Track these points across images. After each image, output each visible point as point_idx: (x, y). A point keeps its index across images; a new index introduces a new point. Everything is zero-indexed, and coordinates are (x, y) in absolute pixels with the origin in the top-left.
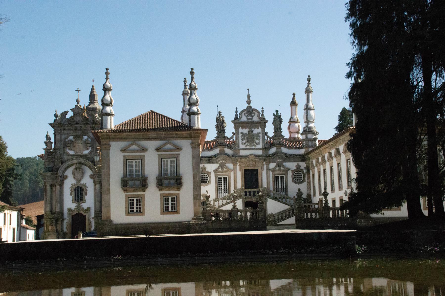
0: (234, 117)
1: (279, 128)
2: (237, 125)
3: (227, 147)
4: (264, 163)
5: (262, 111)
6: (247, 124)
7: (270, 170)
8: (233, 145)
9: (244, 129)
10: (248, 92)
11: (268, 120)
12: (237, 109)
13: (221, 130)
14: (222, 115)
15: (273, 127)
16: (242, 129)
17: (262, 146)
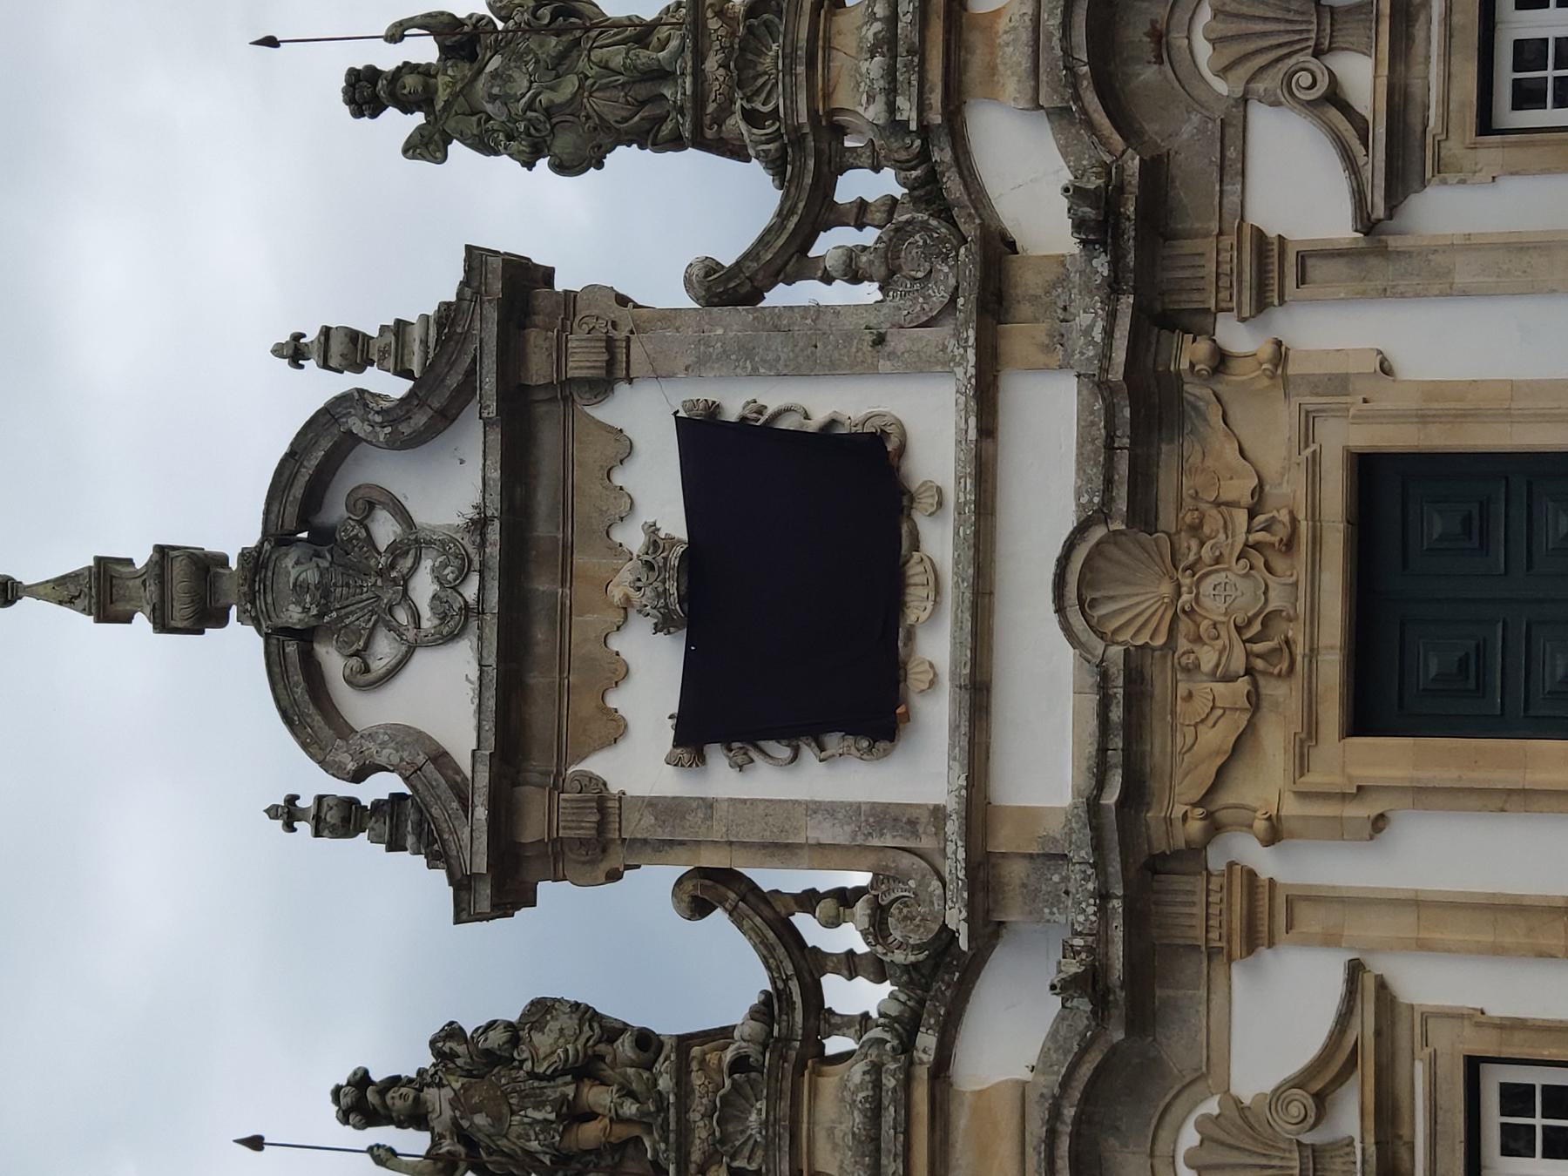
0: (411, 864)
1: (644, 56)
2: (533, 829)
3: (927, 1041)
4: (1236, 336)
5: (325, 365)
6: (540, 633)
7: (1367, 224)
8: (897, 934)
9: (613, 700)
10: (36, 591)
11: (475, 258)
12: (288, 813)
13: (630, 1108)
14: (413, 1059)
15: (623, 158)
16: (614, 730)
17: (920, 366)
